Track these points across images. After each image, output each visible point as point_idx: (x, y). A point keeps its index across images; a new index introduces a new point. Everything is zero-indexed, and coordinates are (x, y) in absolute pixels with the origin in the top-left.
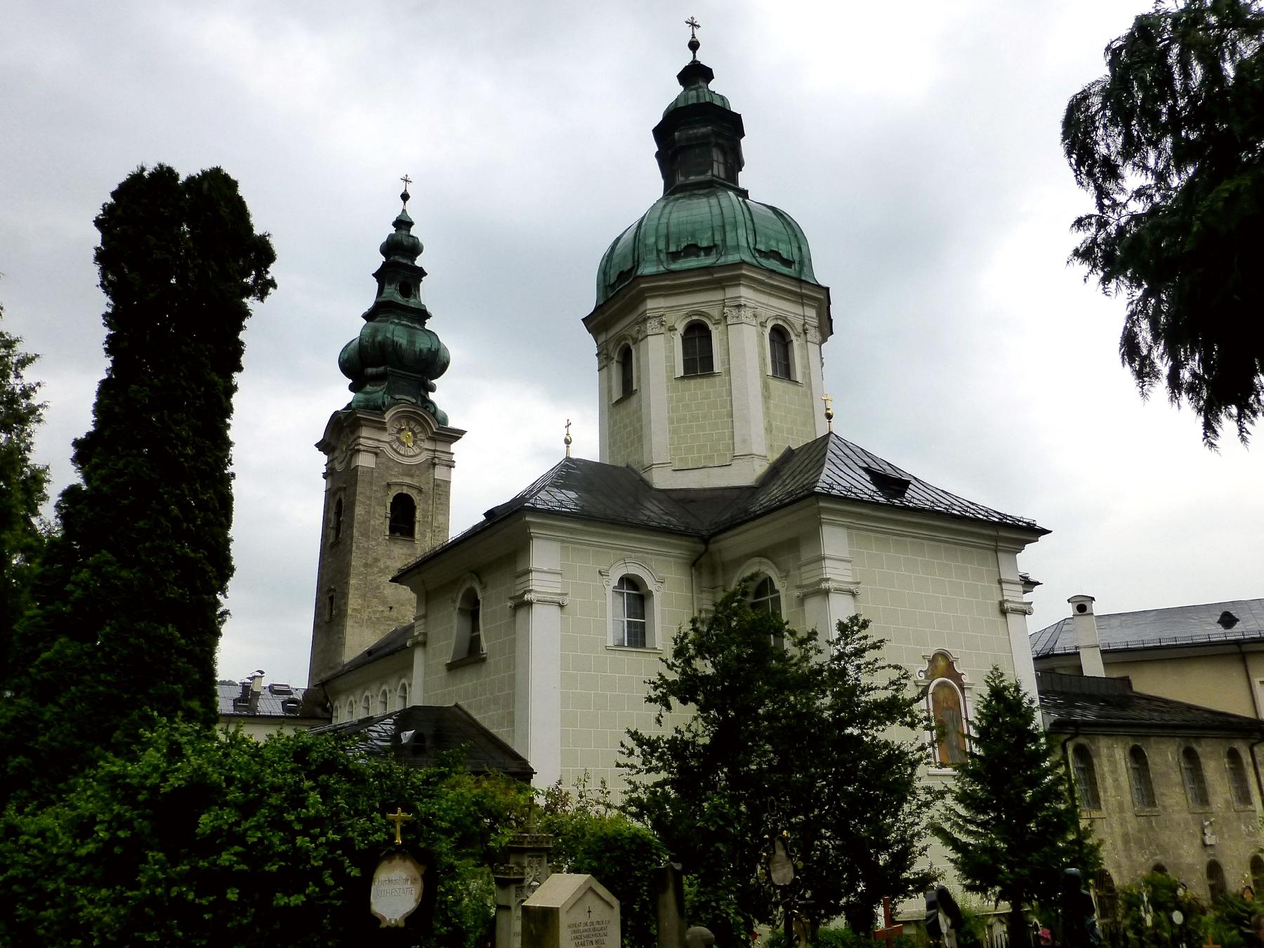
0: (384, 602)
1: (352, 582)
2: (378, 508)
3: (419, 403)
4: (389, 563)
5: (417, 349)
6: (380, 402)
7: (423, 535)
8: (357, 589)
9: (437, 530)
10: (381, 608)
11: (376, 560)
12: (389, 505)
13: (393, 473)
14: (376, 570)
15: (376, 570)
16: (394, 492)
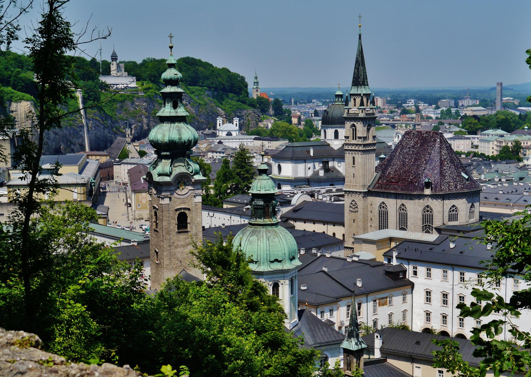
0: (178, 260)
1: (165, 254)
2: (172, 221)
3: (186, 164)
4: (178, 243)
5: (183, 141)
6: (169, 173)
7: (192, 228)
8: (167, 257)
9: (197, 225)
10: (177, 262)
11: (174, 243)
12: (176, 219)
13: (177, 203)
14: (173, 247)
15: (173, 247)
16: (178, 212)
